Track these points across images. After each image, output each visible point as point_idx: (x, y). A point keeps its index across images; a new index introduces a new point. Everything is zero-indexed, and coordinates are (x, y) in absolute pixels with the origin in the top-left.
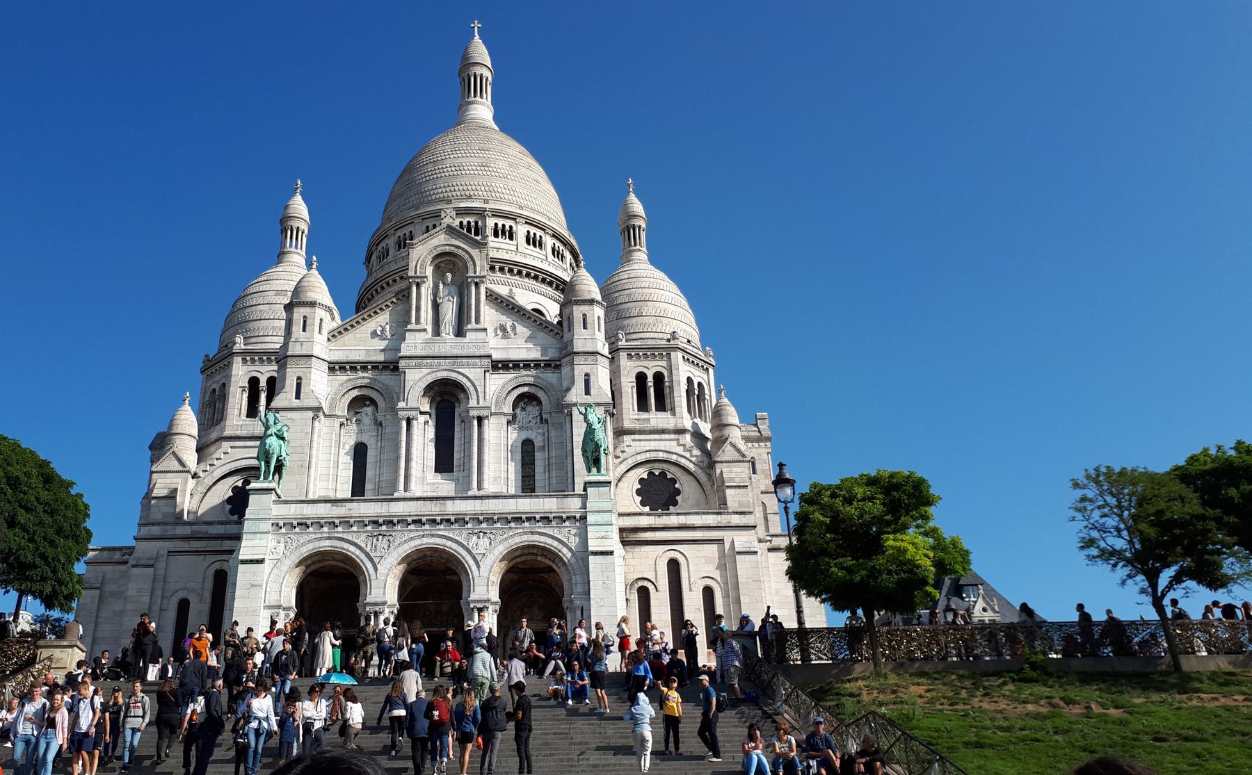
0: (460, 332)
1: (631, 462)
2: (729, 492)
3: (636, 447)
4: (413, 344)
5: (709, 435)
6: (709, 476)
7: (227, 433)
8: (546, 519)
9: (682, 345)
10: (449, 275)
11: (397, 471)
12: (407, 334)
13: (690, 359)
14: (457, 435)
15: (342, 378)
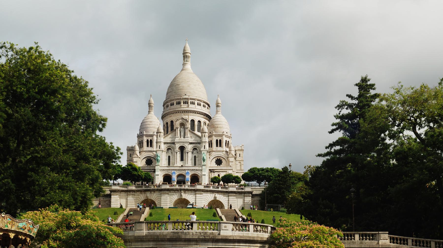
0: (184, 137)
1: (214, 157)
2: (230, 163)
3: (214, 154)
4: (177, 140)
5: (228, 151)
6: (228, 159)
7: (144, 150)
8: (197, 170)
9: (225, 134)
10: (182, 127)
11: (175, 161)
12: (176, 138)
13: (227, 136)
14: (184, 155)
15: (166, 145)
